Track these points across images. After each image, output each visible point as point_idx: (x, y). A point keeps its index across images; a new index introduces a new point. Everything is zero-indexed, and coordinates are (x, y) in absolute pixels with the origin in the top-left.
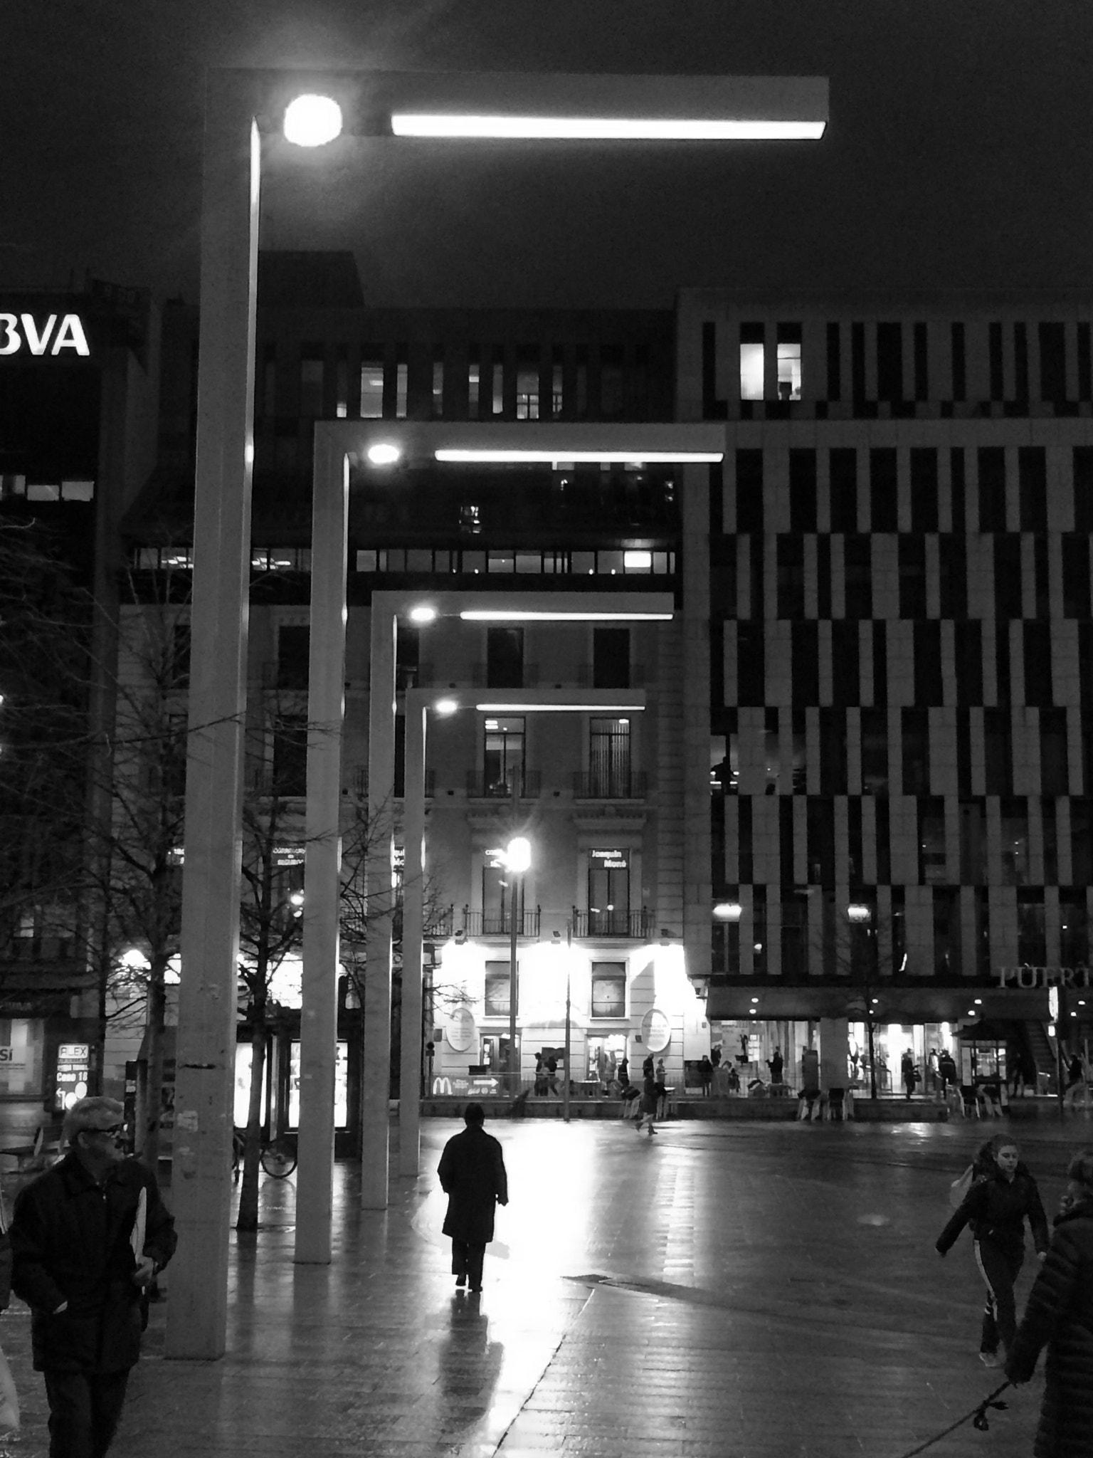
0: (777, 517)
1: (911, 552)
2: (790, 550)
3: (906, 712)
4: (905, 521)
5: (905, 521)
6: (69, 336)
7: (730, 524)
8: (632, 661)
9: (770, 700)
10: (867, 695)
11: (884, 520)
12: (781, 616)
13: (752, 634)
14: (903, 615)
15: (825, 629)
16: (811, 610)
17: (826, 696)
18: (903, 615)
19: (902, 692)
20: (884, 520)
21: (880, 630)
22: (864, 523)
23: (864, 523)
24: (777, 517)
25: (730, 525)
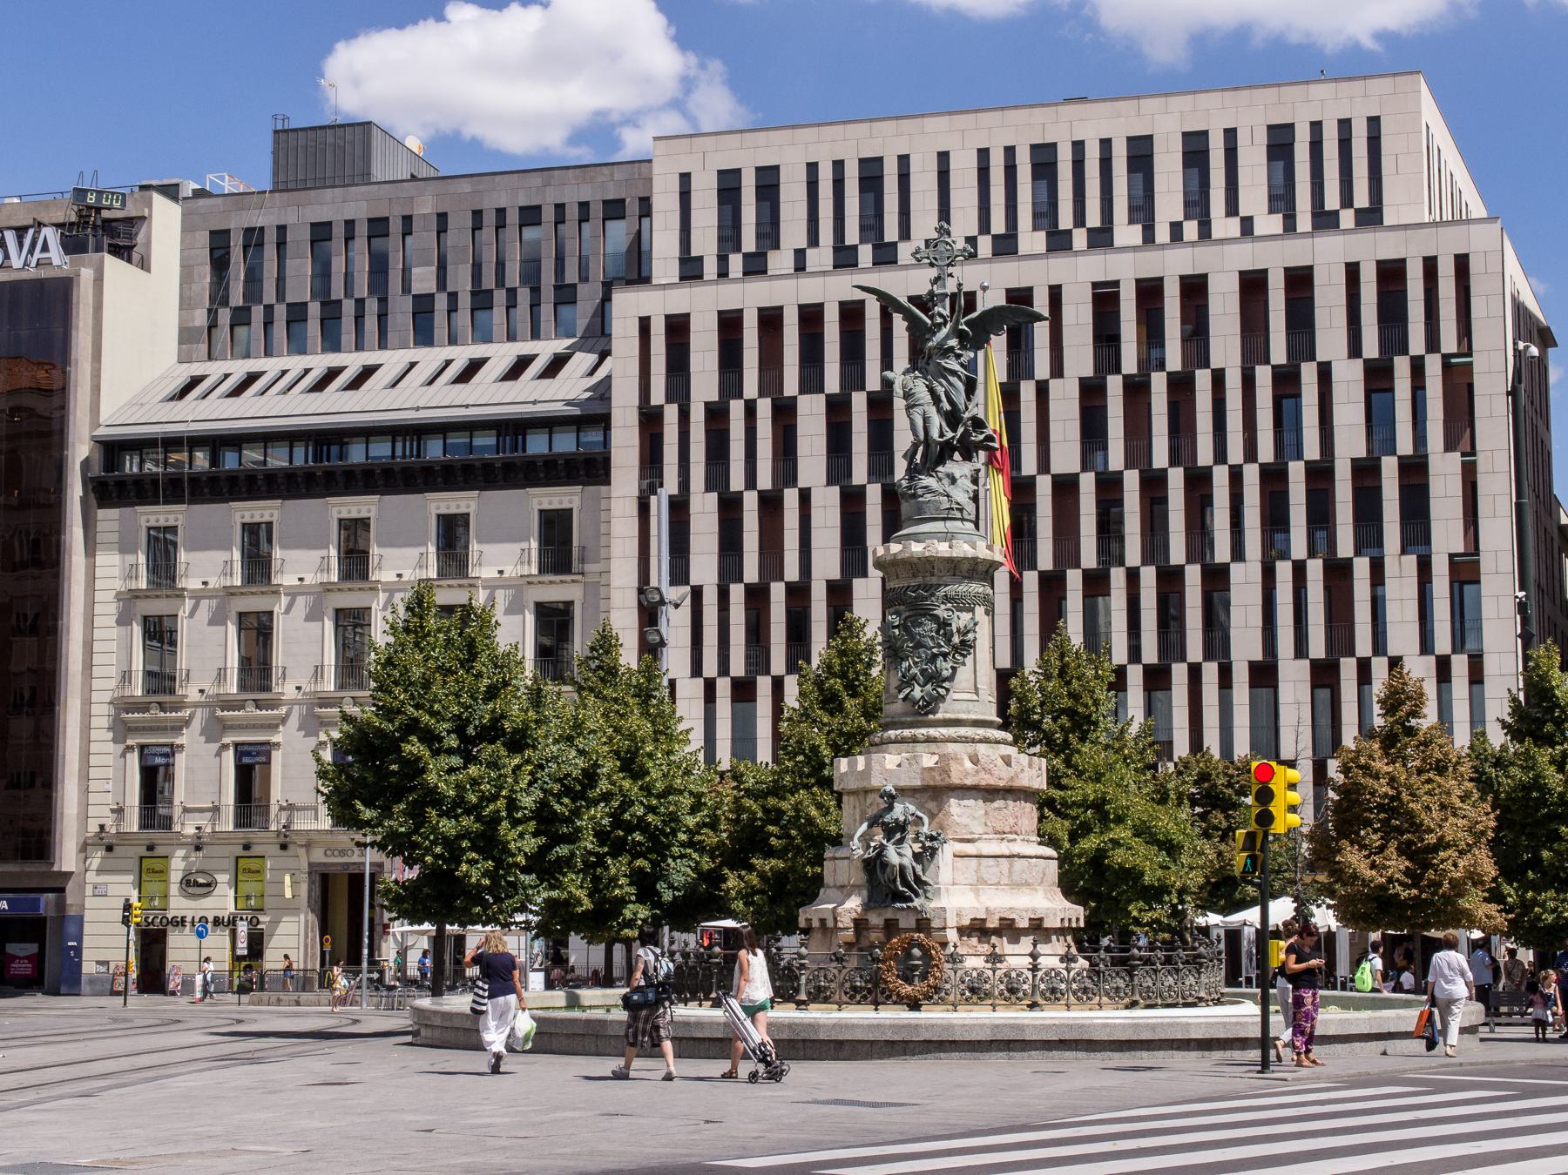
0: (705, 383)
1: (838, 411)
2: (717, 415)
3: (832, 586)
4: (832, 384)
5: (832, 384)
6: (45, 248)
7: (658, 396)
8: (575, 543)
9: (694, 580)
10: (792, 573)
11: (812, 380)
12: (708, 489)
13: (679, 508)
14: (830, 482)
15: (750, 501)
16: (737, 482)
17: (751, 573)
18: (830, 482)
19: (827, 564)
20: (812, 380)
21: (805, 497)
22: (791, 386)
23: (791, 386)
24: (705, 383)
25: (658, 396)
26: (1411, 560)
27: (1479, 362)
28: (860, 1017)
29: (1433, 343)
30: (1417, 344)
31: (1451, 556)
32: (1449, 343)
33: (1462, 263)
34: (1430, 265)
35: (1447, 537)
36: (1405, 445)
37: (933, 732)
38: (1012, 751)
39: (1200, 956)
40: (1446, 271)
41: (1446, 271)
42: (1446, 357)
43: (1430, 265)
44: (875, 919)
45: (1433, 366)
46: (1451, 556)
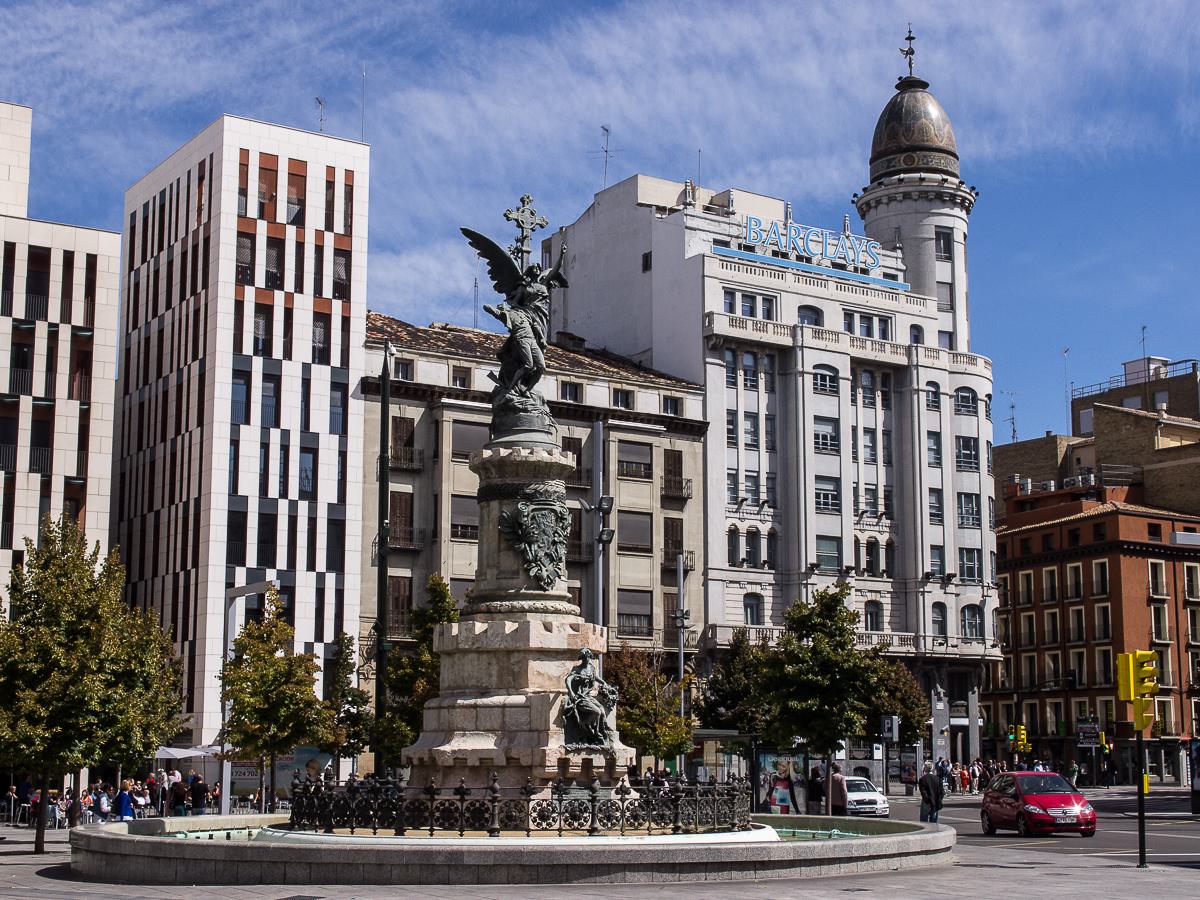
26: (37, 478)
27: (99, 337)
28: (719, 847)
29: (66, 316)
30: (54, 315)
31: (66, 478)
32: (78, 319)
33: (92, 261)
34: (69, 257)
35: (64, 463)
36: (39, 389)
37: (550, 604)
38: (581, 620)
39: (734, 789)
40: (80, 264)
41: (80, 264)
42: (75, 328)
43: (69, 257)
44: (576, 759)
45: (65, 334)
46: (66, 478)
